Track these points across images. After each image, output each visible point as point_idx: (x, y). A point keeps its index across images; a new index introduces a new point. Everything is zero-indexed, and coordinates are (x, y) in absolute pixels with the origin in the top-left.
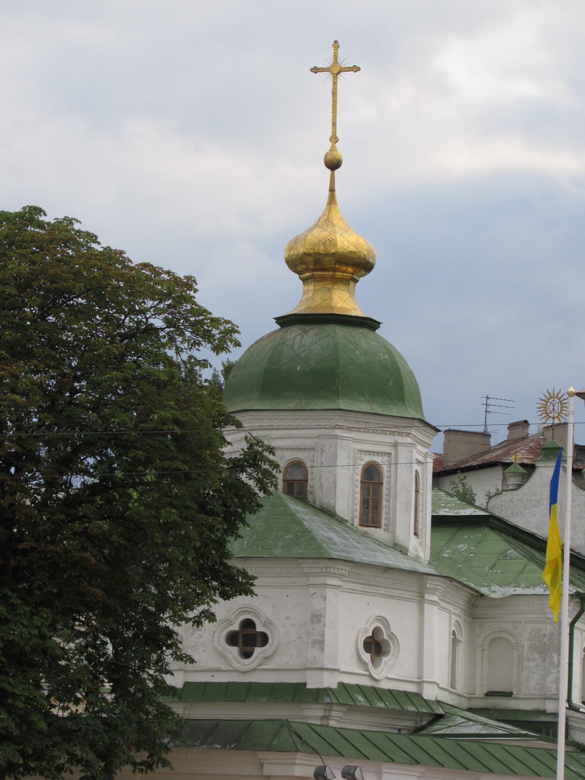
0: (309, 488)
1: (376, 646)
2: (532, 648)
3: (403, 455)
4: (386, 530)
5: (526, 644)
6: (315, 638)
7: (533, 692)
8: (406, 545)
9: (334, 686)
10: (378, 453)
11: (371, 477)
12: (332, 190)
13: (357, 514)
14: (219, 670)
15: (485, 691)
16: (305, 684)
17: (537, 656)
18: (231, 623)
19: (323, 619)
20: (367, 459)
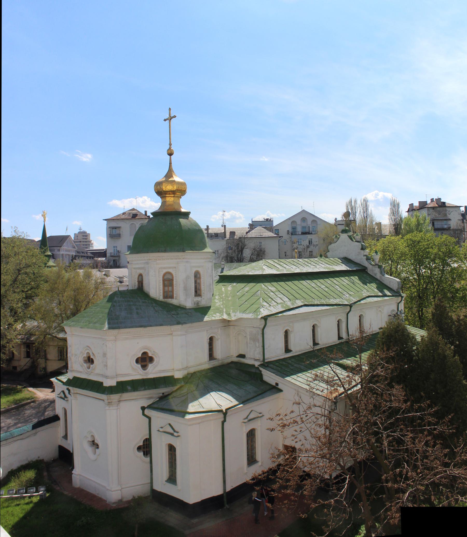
4: (176, 299)
5: (248, 337)
9: (115, 384)
10: (170, 268)
12: (170, 163)
13: (162, 294)
14: (81, 372)
15: (237, 355)
16: (102, 383)
17: (252, 342)
20: (165, 271)
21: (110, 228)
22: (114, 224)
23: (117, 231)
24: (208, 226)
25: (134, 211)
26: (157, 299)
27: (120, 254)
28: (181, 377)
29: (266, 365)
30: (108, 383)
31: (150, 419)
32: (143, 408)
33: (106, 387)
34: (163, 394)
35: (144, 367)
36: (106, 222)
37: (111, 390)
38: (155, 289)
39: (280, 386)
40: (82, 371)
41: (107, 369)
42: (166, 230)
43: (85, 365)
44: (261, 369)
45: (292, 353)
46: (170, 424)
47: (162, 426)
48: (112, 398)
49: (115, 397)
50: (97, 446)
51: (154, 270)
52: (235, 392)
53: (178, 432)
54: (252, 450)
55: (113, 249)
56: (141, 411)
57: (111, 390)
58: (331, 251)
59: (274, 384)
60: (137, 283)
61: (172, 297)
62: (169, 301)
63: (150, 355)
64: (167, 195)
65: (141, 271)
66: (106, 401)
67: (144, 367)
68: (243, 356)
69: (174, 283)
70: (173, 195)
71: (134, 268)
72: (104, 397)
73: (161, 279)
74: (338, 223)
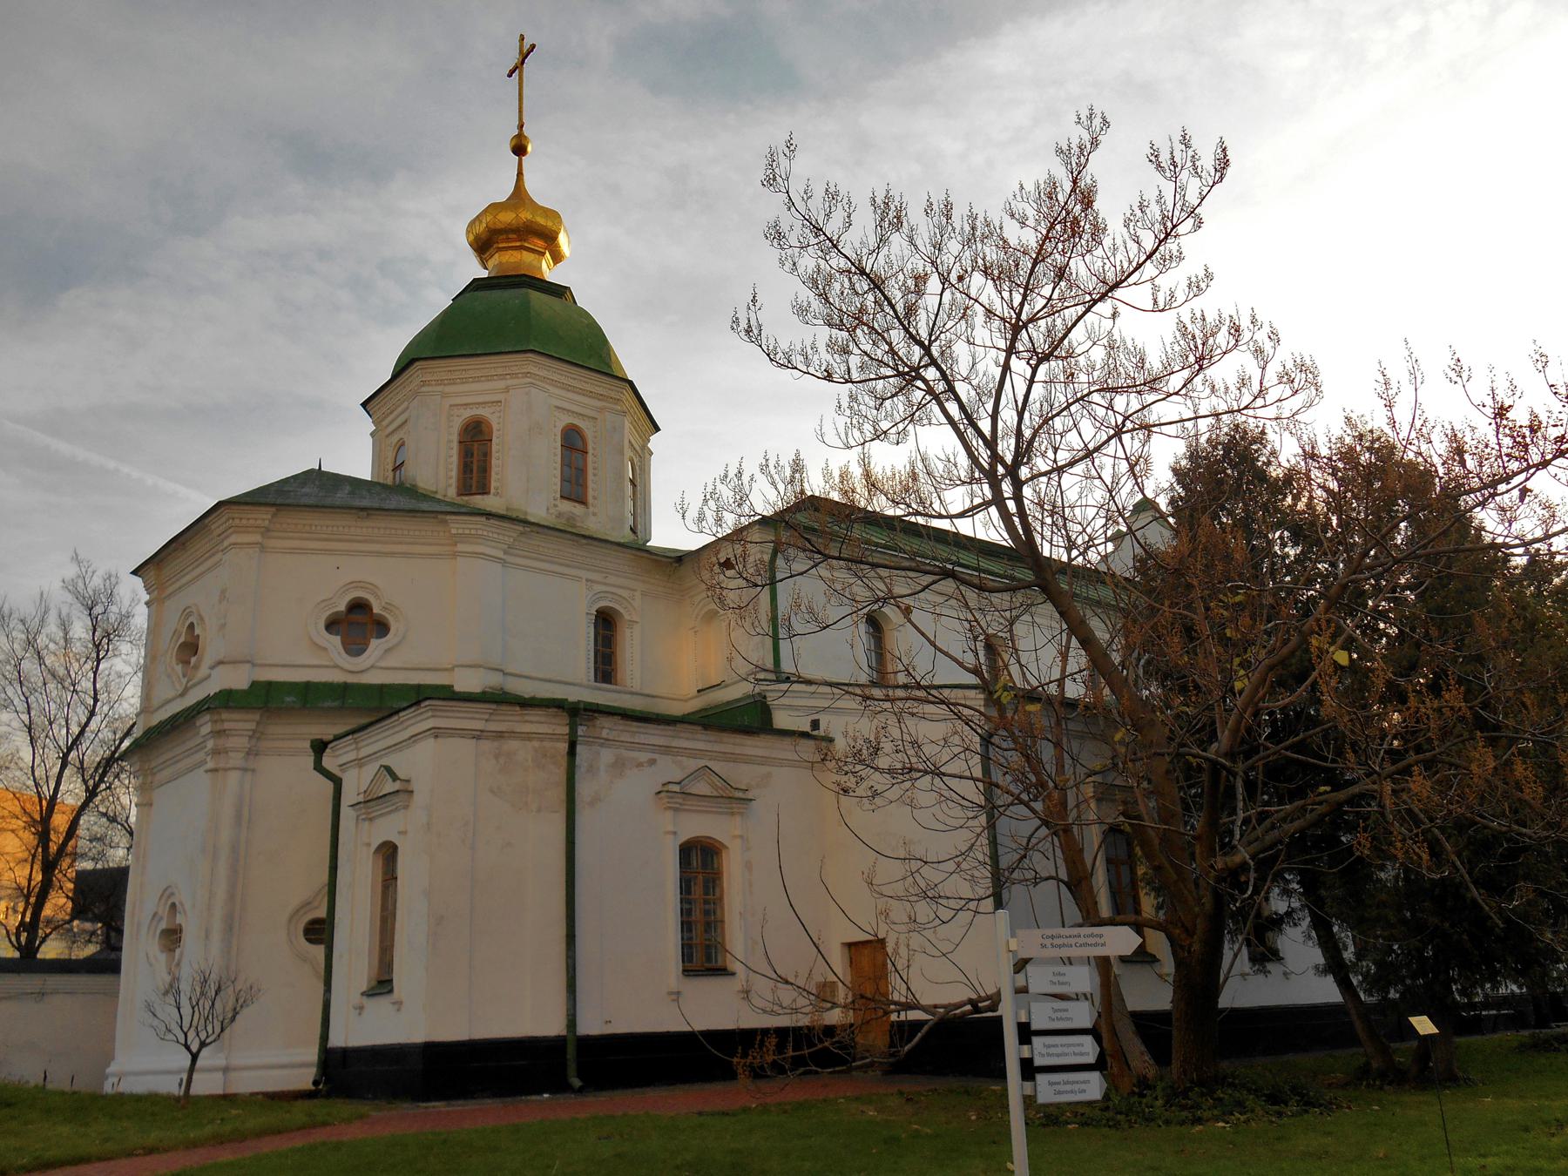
13: (454, 481)
20: (467, 414)
35: (355, 647)
54: (708, 926)
67: (355, 647)
69: (494, 448)
73: (455, 438)
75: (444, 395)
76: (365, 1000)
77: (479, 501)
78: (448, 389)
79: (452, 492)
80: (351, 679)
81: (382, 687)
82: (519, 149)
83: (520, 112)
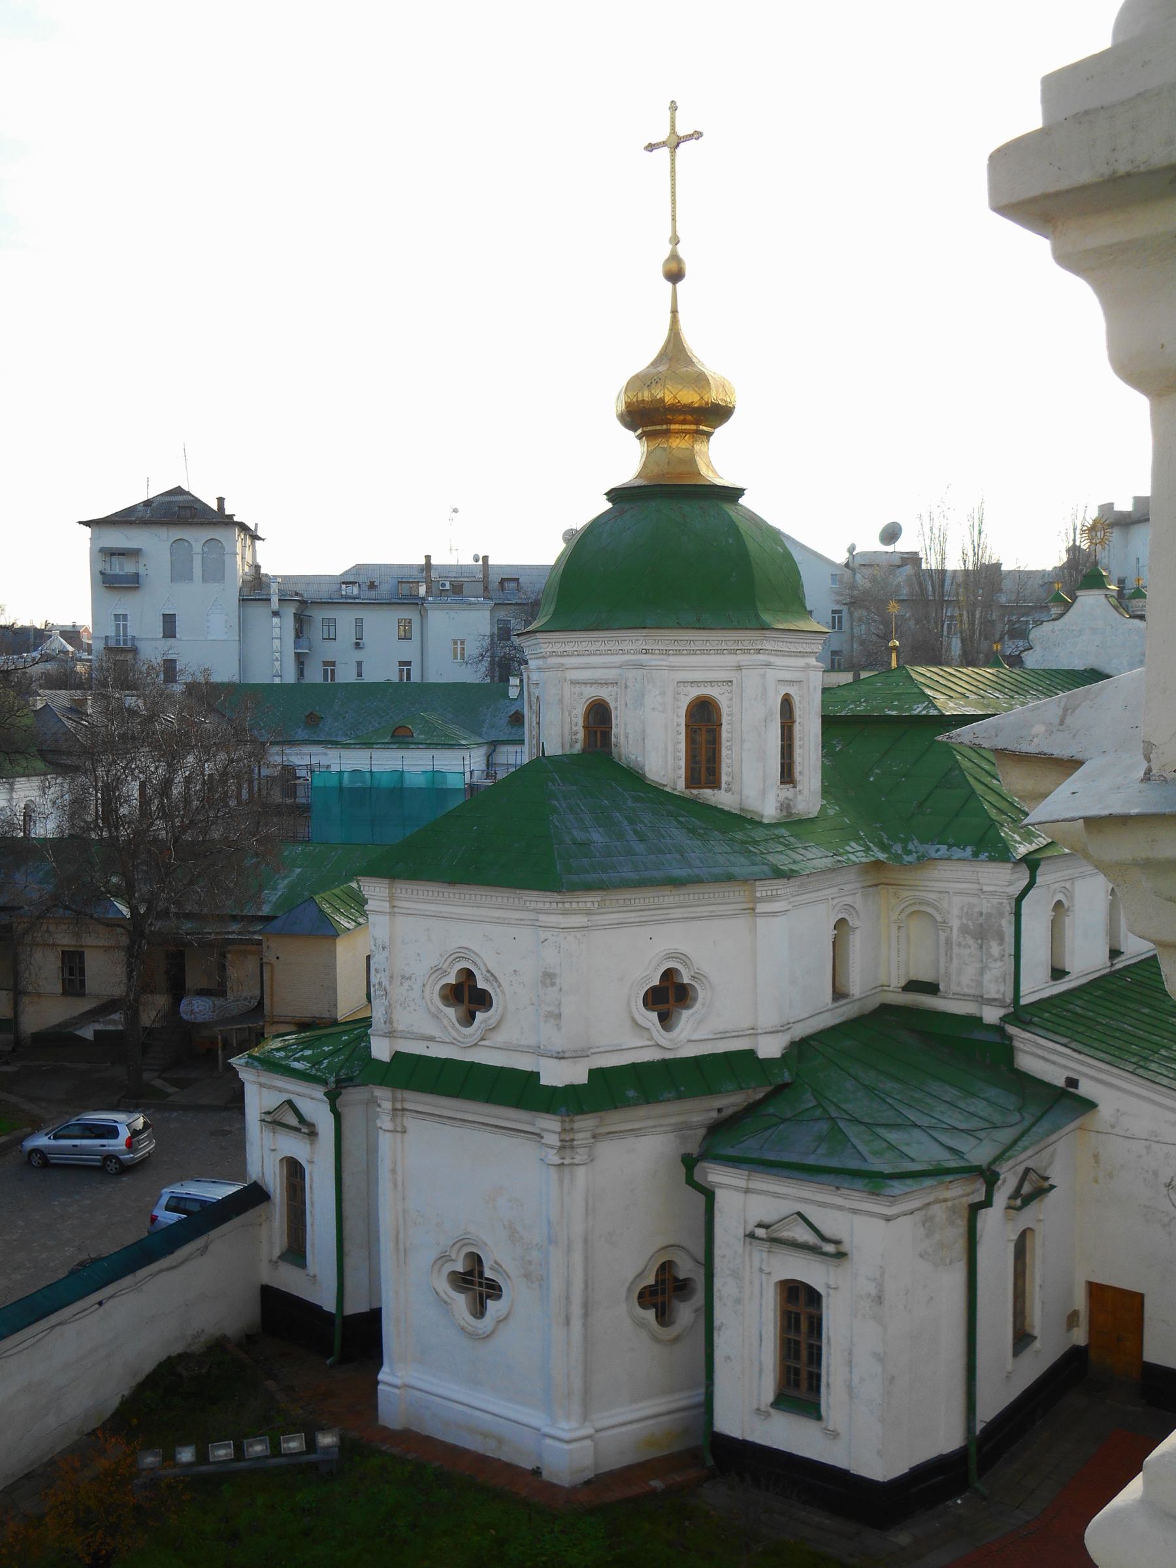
0: (613, 739)
1: (669, 996)
2: (964, 930)
3: (751, 680)
4: (728, 790)
5: (955, 924)
6: (549, 1009)
7: (966, 990)
8: (759, 809)
11: (703, 719)
13: (682, 772)
14: (432, 1039)
15: (903, 983)
16: (535, 1076)
17: (970, 941)
18: (445, 973)
19: (557, 981)
21: (103, 551)
22: (118, 539)
23: (129, 568)
24: (428, 558)
25: (181, 498)
26: (667, 789)
27: (138, 644)
28: (778, 1055)
29: (1021, 1015)
30: (554, 1075)
31: (709, 1195)
32: (689, 1163)
33: (554, 1089)
34: (719, 1110)
36: (88, 530)
37: (568, 1102)
38: (660, 754)
39: (1086, 1089)
40: (436, 1033)
41: (559, 1027)
42: (673, 551)
43: (451, 1012)
44: (1012, 1030)
45: (1067, 978)
46: (799, 1214)
47: (767, 1219)
48: (576, 1126)
49: (585, 1124)
50: (494, 1291)
51: (642, 687)
52: (962, 1105)
53: (837, 1242)
55: (113, 623)
56: (683, 1170)
57: (568, 1102)
58: (1038, 648)
59: (1060, 1082)
60: (581, 735)
61: (715, 784)
62: (708, 795)
63: (686, 980)
64: (673, 427)
65: (604, 693)
66: (553, 1139)
67: (665, 1019)
68: (931, 988)
69: (724, 735)
70: (693, 427)
71: (573, 682)
72: (550, 1124)
74: (858, 561)
75: (672, 668)
76: (772, 1411)
77: (708, 795)
78: (675, 660)
79: (681, 784)
80: (668, 1055)
81: (696, 1059)
82: (675, 275)
83: (674, 219)
